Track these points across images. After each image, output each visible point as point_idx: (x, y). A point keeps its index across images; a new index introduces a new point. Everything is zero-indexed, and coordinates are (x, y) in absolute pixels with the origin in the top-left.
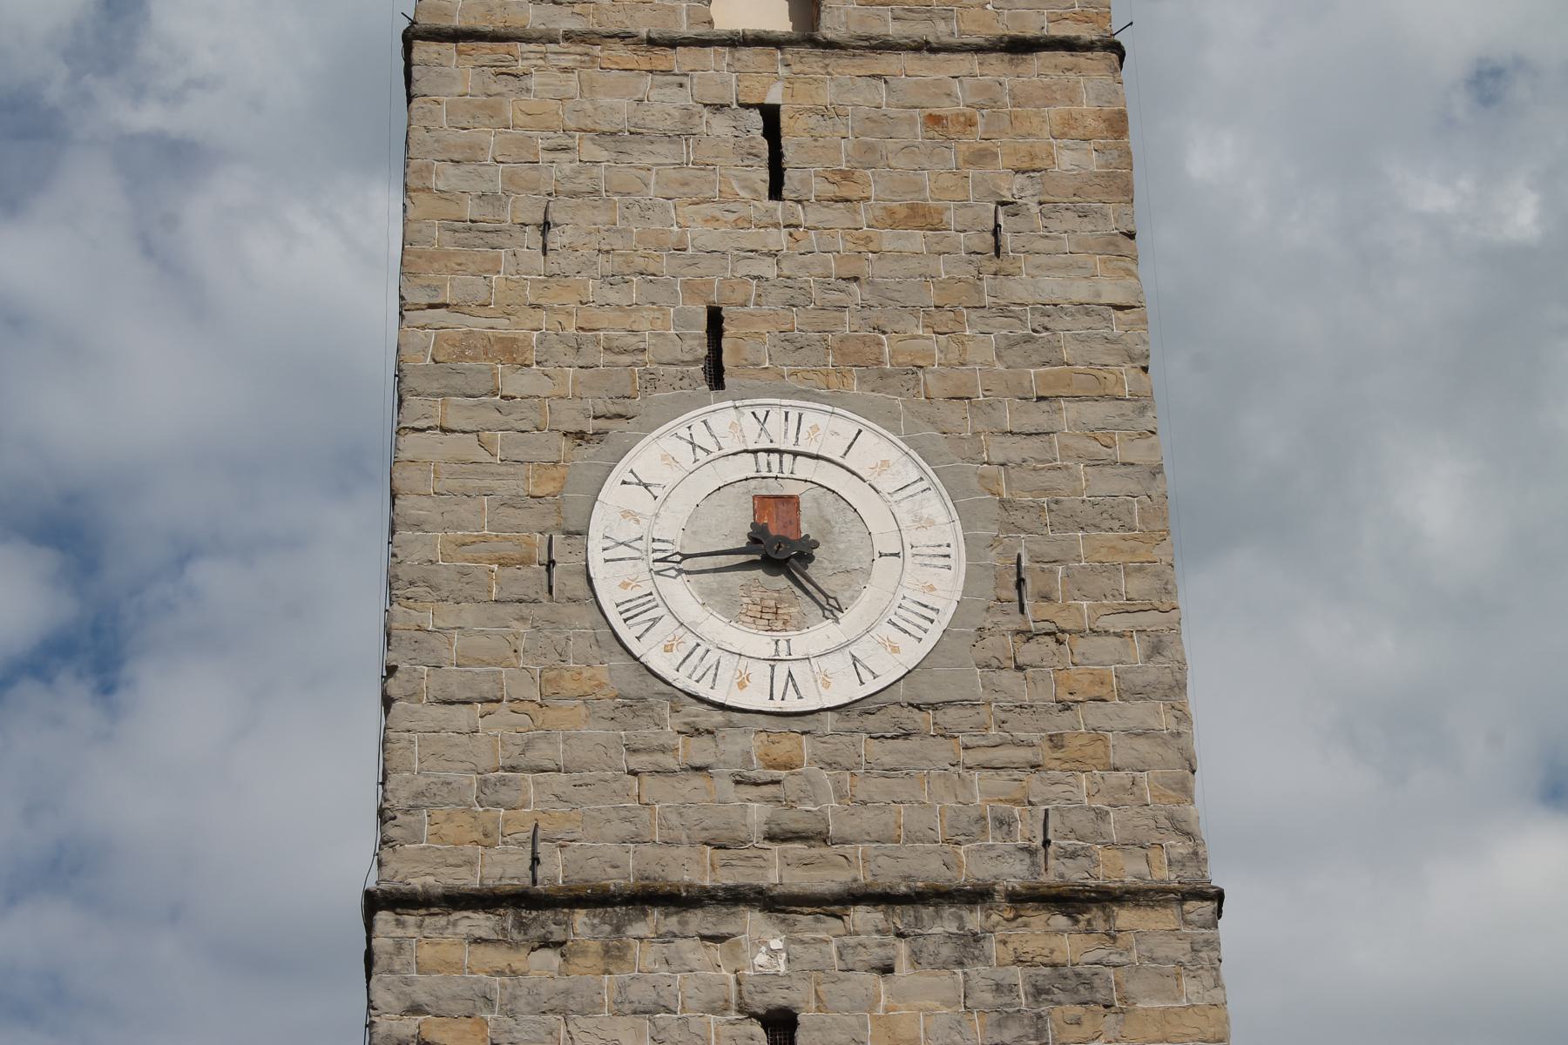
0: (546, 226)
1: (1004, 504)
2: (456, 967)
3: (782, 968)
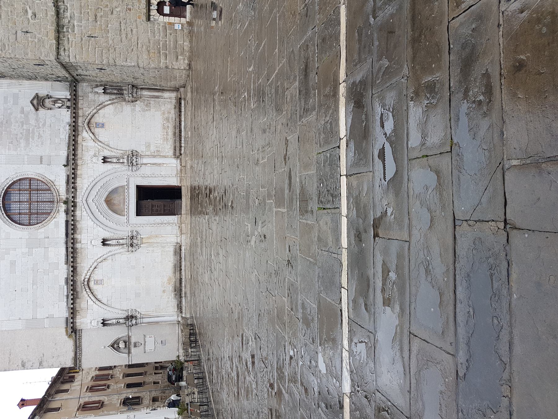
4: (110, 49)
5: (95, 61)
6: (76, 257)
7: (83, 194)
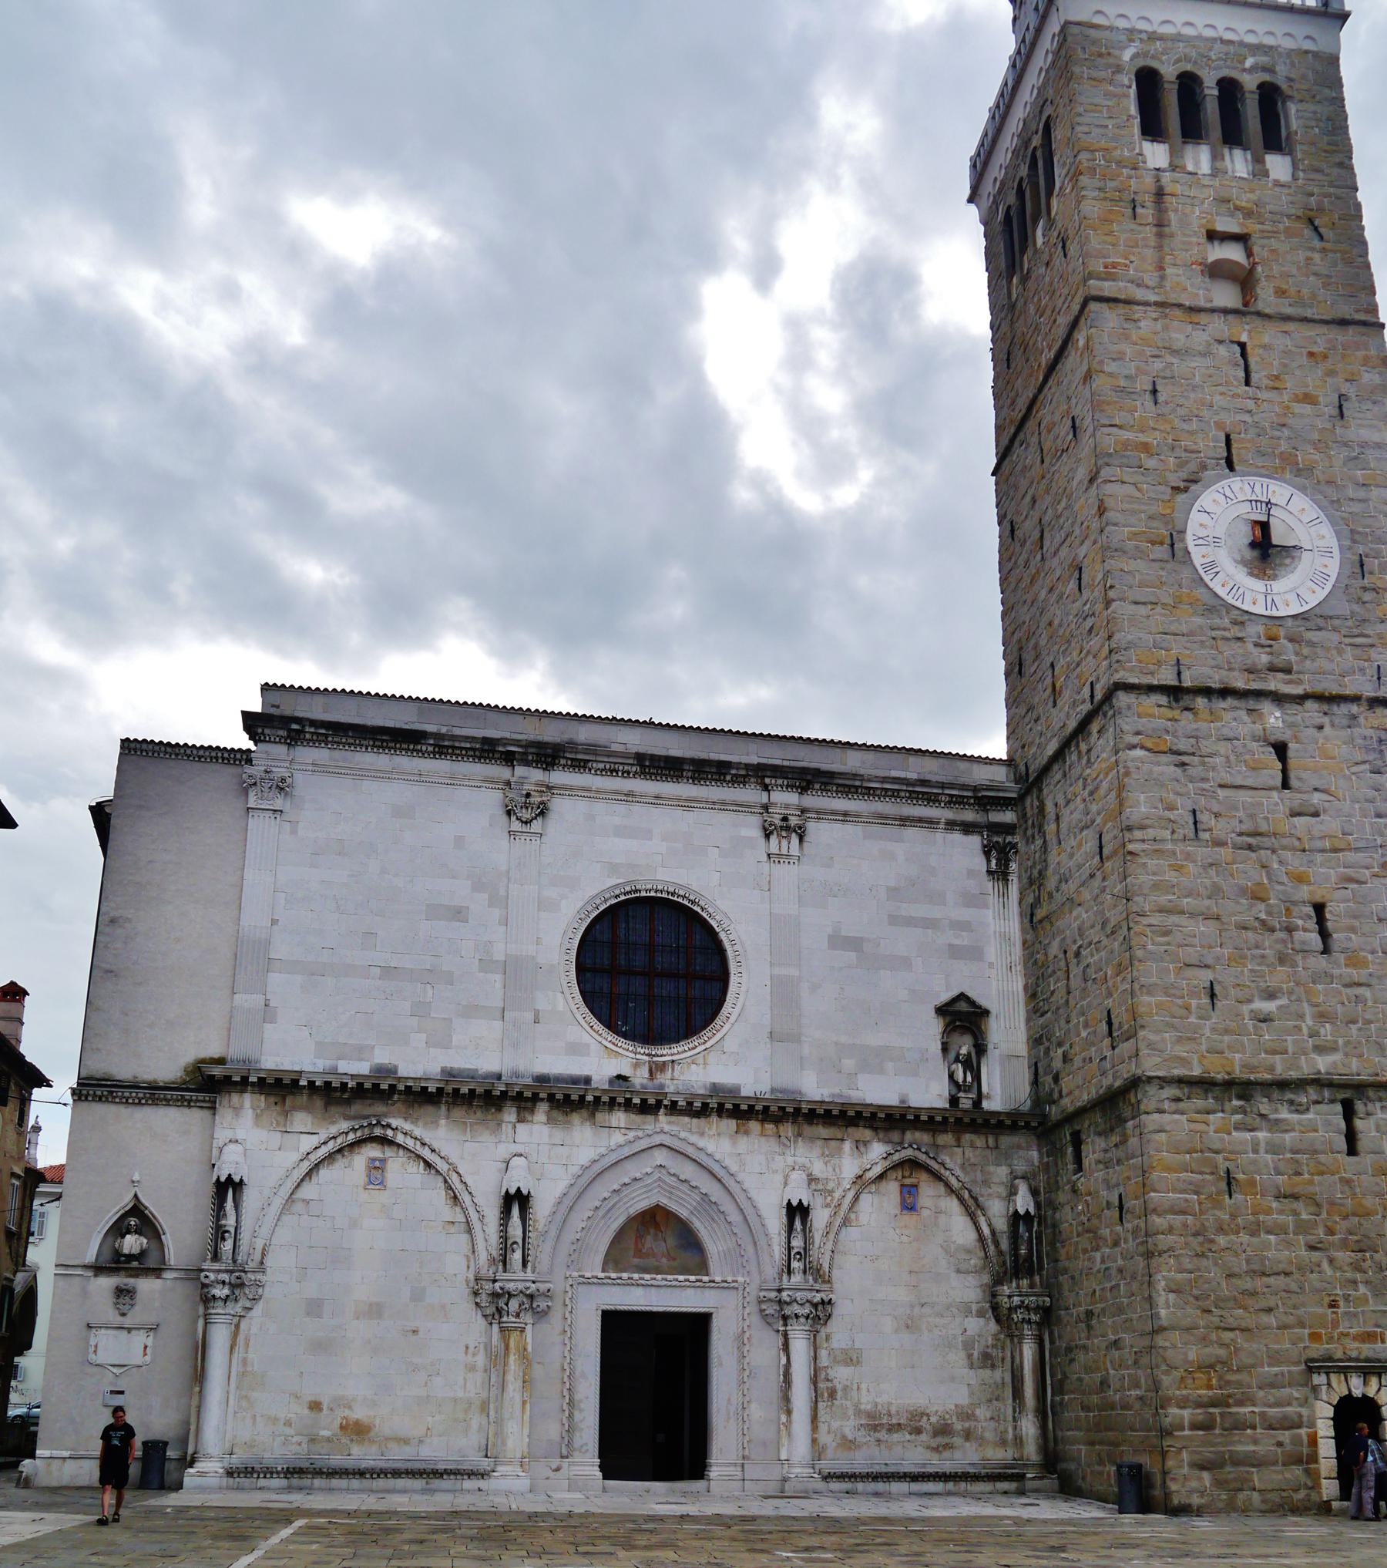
0: (1154, 392)
1: (1352, 531)
2: (1152, 716)
3: (1281, 725)
4: (1200, 1239)
5: (1155, 1191)
6: (470, 1104)
7: (683, 1135)
